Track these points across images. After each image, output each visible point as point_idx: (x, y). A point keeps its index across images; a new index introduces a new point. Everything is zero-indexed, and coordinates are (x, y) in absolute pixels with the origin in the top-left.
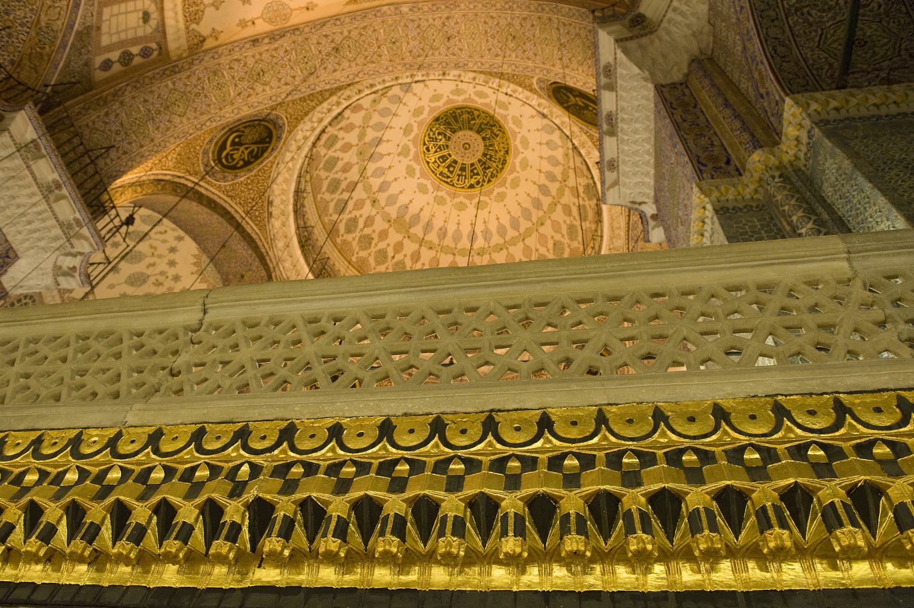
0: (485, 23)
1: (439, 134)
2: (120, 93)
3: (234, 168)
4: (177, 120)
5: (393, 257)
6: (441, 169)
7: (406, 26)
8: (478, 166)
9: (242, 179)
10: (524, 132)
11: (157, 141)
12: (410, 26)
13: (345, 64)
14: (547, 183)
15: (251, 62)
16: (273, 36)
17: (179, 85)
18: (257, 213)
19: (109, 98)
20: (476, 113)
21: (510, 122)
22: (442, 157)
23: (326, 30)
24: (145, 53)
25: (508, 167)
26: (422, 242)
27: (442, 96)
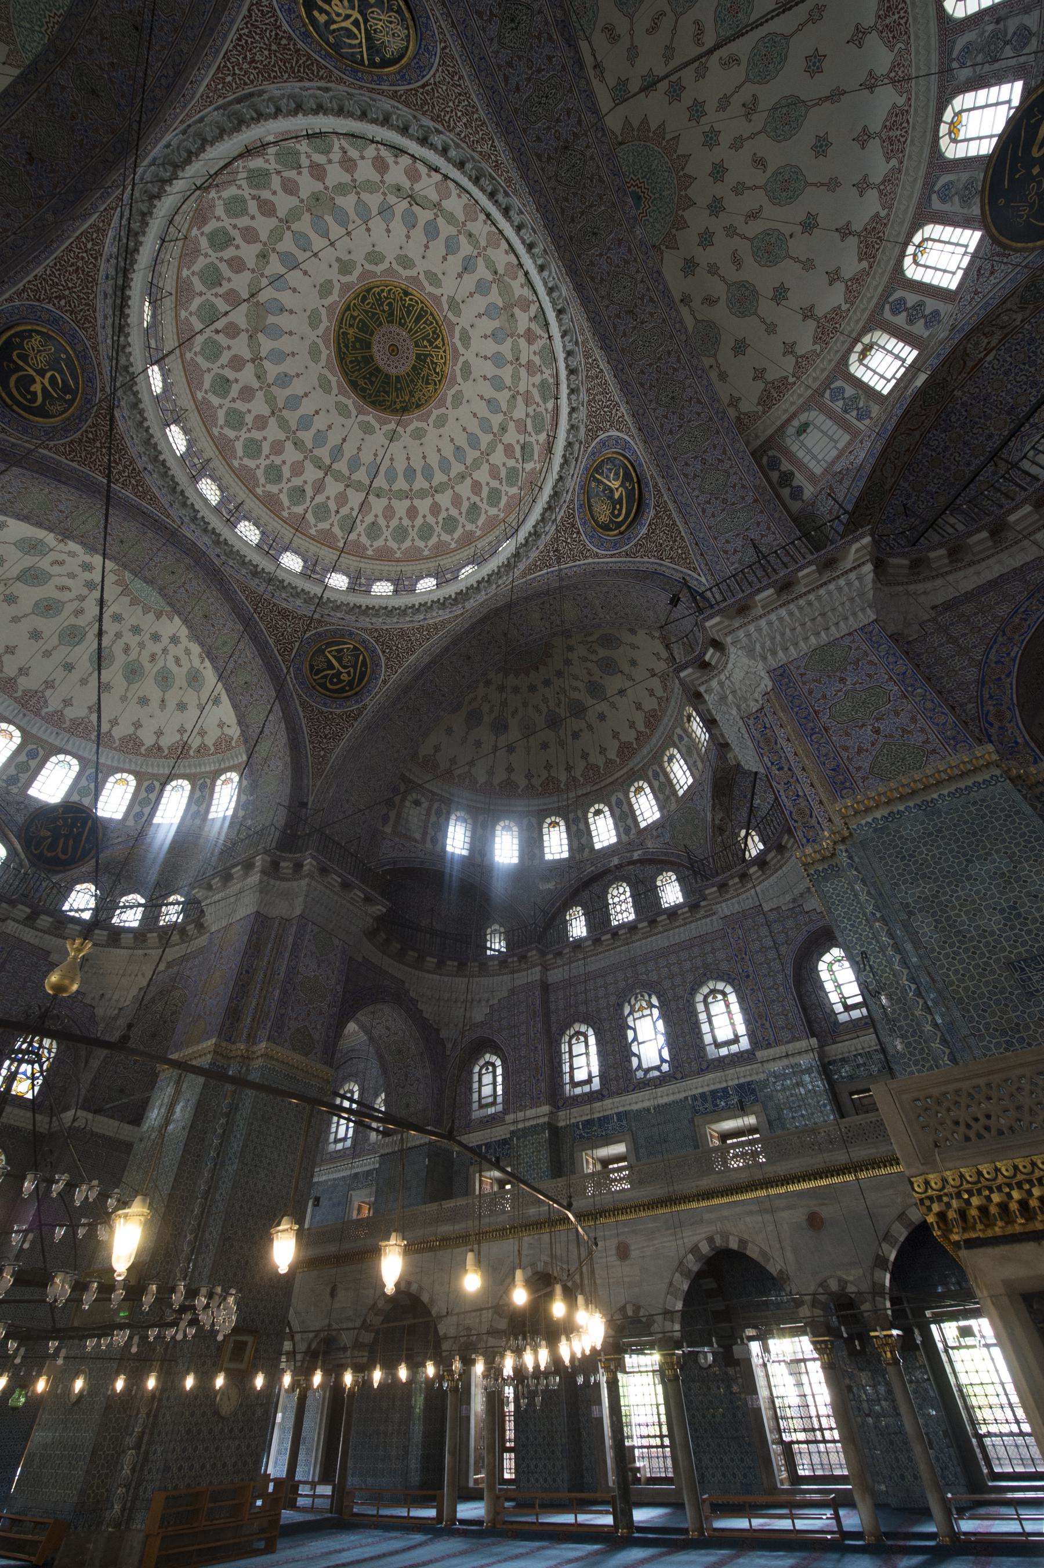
1: (390, 304)
6: (351, 331)
7: (620, 241)
9: (286, 27)
10: (452, 413)
18: (229, 79)
20: (438, 342)
22: (365, 325)
27: (440, 287)
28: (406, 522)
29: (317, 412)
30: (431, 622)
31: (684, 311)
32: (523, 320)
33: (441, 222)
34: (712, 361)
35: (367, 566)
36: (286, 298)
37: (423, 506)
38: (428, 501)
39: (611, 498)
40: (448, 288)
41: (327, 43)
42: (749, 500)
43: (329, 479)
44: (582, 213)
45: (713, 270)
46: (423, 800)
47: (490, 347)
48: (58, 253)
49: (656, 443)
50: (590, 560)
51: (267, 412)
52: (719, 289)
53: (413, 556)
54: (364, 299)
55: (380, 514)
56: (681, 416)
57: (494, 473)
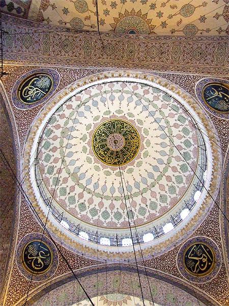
0: (185, 47)
1: (103, 133)
2: (7, 18)
3: (25, 100)
5: (69, 193)
6: (100, 151)
9: (24, 110)
10: (149, 137)
12: (142, 45)
13: (105, 56)
14: (158, 165)
15: (63, 38)
20: (125, 125)
21: (143, 131)
24: (19, 10)
25: (137, 155)
26: (85, 188)
28: (170, 184)
29: (113, 184)
30: (212, 206)
31: (176, 34)
32: (140, 91)
33: (95, 99)
34: (199, 32)
35: (173, 212)
36: (78, 164)
37: (170, 172)
38: (170, 169)
39: (220, 99)
40: (113, 109)
41: (35, 101)
44: (123, 53)
47: (140, 108)
48: (19, 218)
49: (212, 69)
51: (100, 200)
53: (184, 192)
55: (160, 191)
56: (210, 54)
57: (179, 137)
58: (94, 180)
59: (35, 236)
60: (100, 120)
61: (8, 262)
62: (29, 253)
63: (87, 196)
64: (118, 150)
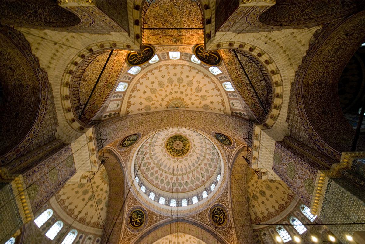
4: (119, 133)
7: (180, 115)
8: (181, 151)
11: (113, 138)
13: (163, 123)
15: (140, 120)
16: (147, 114)
17: (122, 124)
19: (105, 125)
20: (182, 137)
23: (160, 114)
25: (189, 152)
26: (163, 171)
28: (206, 167)
30: (225, 188)
36: (159, 158)
42: (239, 125)
43: (189, 175)
45: (196, 100)
46: (265, 232)
50: (234, 152)
52: (199, 101)
54: (168, 145)
58: (168, 166)
59: (135, 207)
60: (169, 135)
61: (121, 226)
62: (132, 218)
63: (164, 175)
64: (179, 149)
